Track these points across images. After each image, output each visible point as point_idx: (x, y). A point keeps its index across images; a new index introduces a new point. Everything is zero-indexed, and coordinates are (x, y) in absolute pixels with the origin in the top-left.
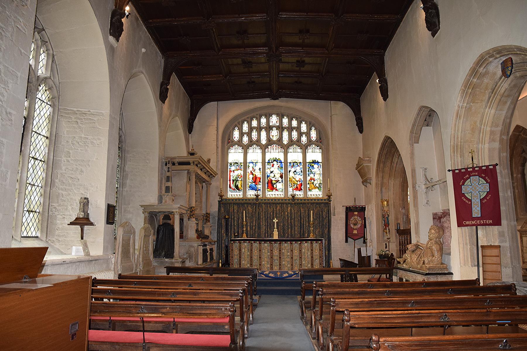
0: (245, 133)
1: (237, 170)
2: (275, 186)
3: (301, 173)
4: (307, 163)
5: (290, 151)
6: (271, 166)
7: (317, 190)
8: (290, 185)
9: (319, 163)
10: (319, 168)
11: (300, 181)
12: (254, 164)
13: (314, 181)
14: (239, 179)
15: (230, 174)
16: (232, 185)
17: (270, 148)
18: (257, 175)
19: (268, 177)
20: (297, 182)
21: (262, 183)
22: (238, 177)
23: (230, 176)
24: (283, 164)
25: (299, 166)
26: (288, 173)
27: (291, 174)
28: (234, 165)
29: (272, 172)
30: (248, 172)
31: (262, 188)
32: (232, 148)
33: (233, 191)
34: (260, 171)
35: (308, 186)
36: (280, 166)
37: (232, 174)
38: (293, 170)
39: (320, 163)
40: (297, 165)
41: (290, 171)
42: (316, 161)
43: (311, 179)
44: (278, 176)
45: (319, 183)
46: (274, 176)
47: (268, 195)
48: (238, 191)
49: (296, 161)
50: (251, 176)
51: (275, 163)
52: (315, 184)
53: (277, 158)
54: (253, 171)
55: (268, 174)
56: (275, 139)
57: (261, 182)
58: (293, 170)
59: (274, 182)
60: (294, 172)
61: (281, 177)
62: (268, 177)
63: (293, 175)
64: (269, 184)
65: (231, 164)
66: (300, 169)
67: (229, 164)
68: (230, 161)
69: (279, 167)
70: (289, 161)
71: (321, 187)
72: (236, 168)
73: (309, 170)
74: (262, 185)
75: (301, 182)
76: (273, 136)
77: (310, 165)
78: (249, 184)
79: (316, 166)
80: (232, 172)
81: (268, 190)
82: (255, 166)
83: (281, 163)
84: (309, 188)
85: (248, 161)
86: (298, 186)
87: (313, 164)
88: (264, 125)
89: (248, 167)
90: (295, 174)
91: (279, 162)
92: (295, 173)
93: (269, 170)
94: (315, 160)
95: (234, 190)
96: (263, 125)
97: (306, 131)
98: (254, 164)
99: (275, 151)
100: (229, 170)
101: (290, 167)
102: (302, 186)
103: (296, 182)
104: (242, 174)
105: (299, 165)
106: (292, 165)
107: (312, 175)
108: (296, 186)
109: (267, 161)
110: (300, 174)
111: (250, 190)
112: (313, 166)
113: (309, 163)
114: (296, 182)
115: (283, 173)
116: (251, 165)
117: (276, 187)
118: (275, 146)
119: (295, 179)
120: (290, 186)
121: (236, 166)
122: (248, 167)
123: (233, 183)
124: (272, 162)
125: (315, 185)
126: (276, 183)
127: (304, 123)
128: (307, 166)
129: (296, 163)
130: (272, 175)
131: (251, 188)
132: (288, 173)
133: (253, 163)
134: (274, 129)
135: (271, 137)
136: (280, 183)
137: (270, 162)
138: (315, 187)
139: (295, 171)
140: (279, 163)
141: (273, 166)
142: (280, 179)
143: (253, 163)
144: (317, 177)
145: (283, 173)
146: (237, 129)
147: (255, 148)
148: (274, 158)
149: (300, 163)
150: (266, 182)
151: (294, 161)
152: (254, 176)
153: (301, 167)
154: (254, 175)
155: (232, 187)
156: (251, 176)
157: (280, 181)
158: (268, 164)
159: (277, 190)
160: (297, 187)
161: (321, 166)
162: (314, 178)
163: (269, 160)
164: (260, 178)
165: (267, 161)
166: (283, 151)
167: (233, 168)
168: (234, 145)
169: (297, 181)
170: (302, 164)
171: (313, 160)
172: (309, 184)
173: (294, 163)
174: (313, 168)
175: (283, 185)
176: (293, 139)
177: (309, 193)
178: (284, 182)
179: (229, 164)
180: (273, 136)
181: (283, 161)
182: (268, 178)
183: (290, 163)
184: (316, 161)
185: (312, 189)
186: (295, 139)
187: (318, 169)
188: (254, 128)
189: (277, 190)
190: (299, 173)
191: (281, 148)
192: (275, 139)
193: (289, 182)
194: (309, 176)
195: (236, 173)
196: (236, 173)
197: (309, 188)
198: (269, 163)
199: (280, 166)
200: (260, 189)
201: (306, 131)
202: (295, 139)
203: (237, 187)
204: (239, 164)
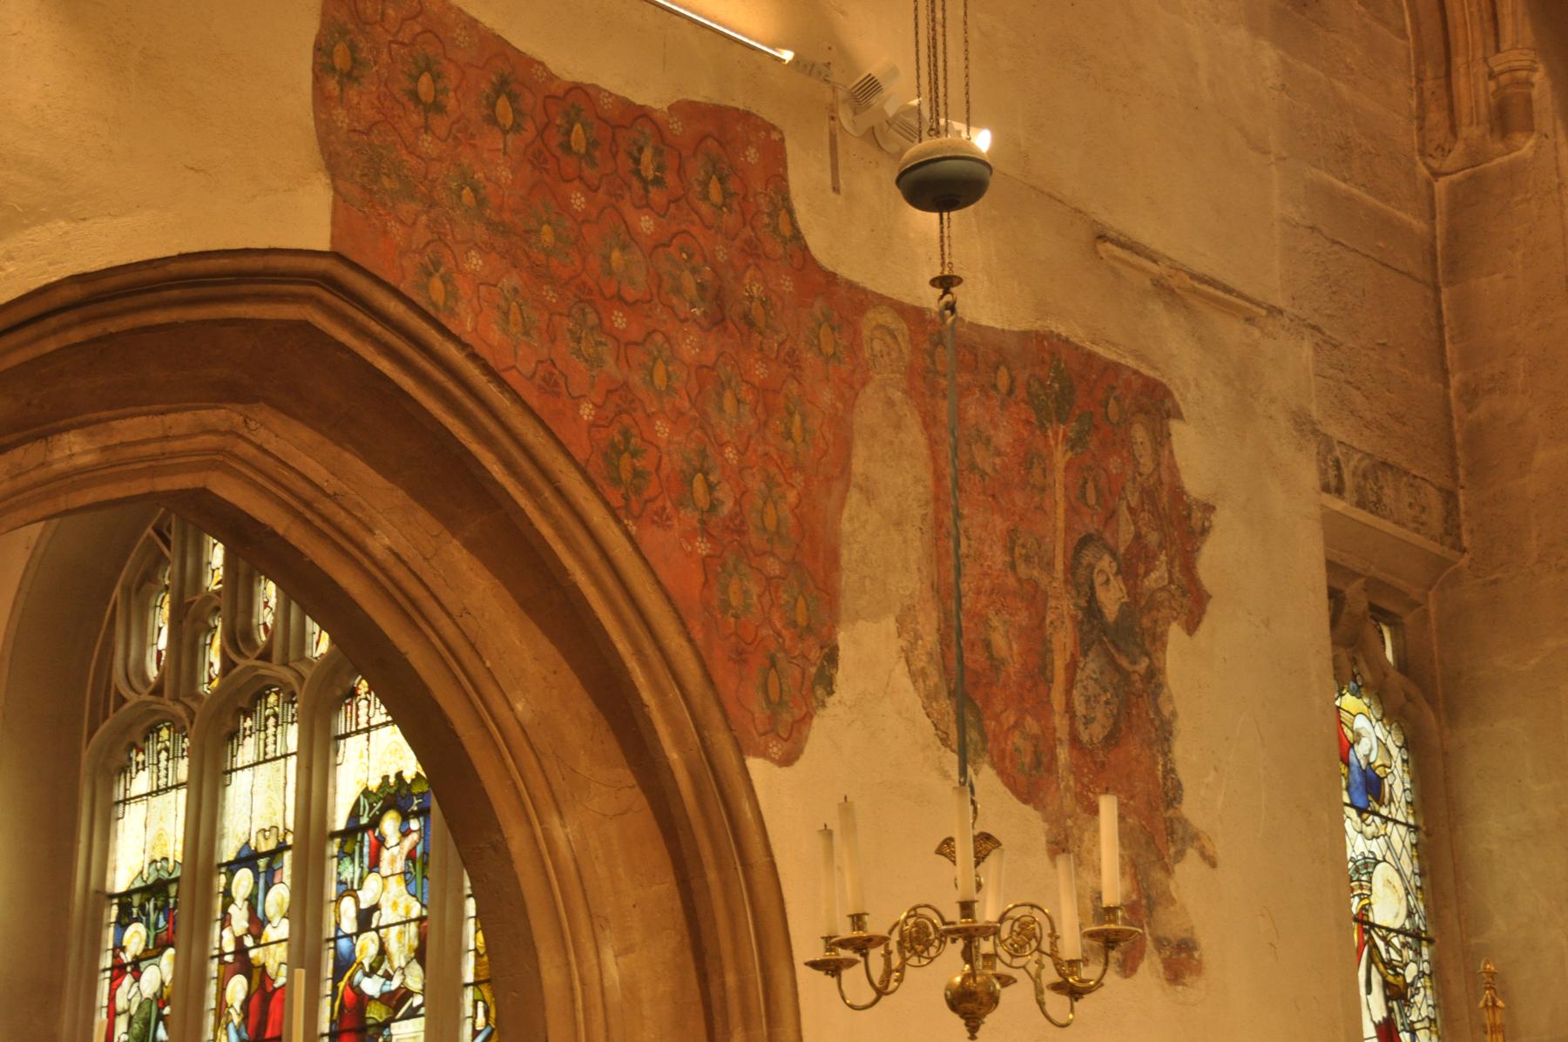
8: (481, 1020)
12: (262, 863)
15: (112, 998)
23: (113, 1014)
28: (142, 907)
32: (141, 757)
37: (127, 995)
44: (401, 943)
46: (383, 952)
54: (249, 942)
59: (375, 1013)
69: (411, 856)
72: (152, 934)
80: (128, 979)
98: (262, 863)
100: (107, 961)
116: (244, 880)
121: (153, 917)
126: (386, 1024)
136: (413, 1013)
147: (272, 721)
152: (255, 986)
156: (238, 988)
163: (355, 814)
167: (136, 938)
182: (342, 985)
198: (353, 831)
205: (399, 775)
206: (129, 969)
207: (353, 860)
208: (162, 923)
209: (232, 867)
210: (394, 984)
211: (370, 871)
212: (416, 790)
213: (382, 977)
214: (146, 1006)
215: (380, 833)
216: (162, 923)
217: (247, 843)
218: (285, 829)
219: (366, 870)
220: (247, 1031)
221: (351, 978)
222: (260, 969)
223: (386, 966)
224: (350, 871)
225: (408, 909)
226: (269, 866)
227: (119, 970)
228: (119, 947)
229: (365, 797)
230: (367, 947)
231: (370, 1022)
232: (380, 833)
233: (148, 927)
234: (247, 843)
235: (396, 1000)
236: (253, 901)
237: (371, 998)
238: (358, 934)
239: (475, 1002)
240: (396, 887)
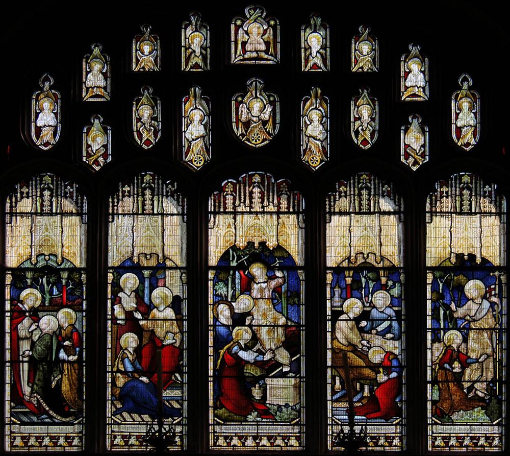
0: (94, 109)
1: (54, 307)
2: (256, 393)
3: (395, 324)
4: (430, 277)
5: (343, 204)
6: (238, 287)
7: (478, 414)
8: (338, 385)
9: (494, 268)
10: (494, 299)
11: (388, 370)
13: (465, 365)
14: (62, 355)
15: (14, 328)
16: (27, 390)
17: (229, 189)
18: (159, 332)
19: (220, 341)
20: (372, 375)
21: (186, 377)
22: (60, 346)
23: (16, 339)
24: (302, 275)
25: (385, 287)
26: (329, 324)
27: (344, 331)
29: (239, 319)
30: (114, 319)
31: (185, 404)
33: (35, 419)
34: (177, 310)
35: (432, 393)
36: (284, 289)
37: (25, 325)
38: (354, 306)
39: (497, 273)
40: (378, 279)
41: (336, 315)
42: (479, 260)
43: (450, 355)
45: (490, 376)
46: (255, 339)
47: (221, 441)
48: (59, 418)
49: (371, 260)
50: (130, 340)
51: (257, 270)
52: (466, 385)
53: (271, 243)
54: (138, 316)
55: (222, 330)
56: (257, 139)
57: (185, 369)
58: (354, 306)
60: (357, 320)
61: (290, 344)
62: (220, 341)
63: (355, 338)
64: (227, 384)
65: (18, 273)
66: (391, 306)
67: (9, 279)
68: (12, 261)
69: (277, 290)
70: (333, 258)
71: (500, 402)
73: (435, 310)
74: (185, 388)
75: (394, 375)
76: (247, 124)
77: (447, 284)
78: (121, 381)
79: (473, 287)
80: (26, 322)
81: (221, 412)
82: (152, 288)
83: (288, 264)
84: (434, 402)
85: (114, 260)
86: (379, 393)
87: (462, 278)
88: (200, 62)
89: (115, 294)
90: (362, 330)
91: (281, 268)
92: (364, 323)
93: (222, 307)
94: (472, 257)
95: (39, 411)
96: (193, 62)
97: (423, 97)
98: (146, 273)
99: (257, 208)
101: (337, 291)
102: (399, 393)
103: (367, 372)
104: (82, 325)
105: (384, 280)
106: (349, 280)
107: (454, 337)
108: (366, 393)
109: (213, 261)
110: (389, 329)
111: (125, 414)
112: (460, 288)
113: (438, 274)
114: (367, 372)
115: (298, 325)
116: (130, 281)
117: (264, 397)
118: (257, 179)
119: (363, 355)
120: (334, 392)
122: (115, 294)
123: (31, 381)
124: (241, 267)
125: (470, 389)
126: (263, 377)
127: (414, 50)
128: (429, 288)
129: (374, 270)
130: (243, 334)
131: (131, 405)
132: (329, 324)
133: (136, 269)
134: (254, 84)
135: (239, 132)
136: (283, 375)
137: (234, 264)
138: (470, 402)
139: (365, 315)
140: (279, 274)
141: (246, 289)
142: (283, 356)
143: (136, 269)
144: (477, 345)
145: (303, 322)
146: (47, 84)
148: (251, 244)
149: (392, 270)
150: (211, 373)
151: (360, 260)
152: (145, 341)
153: (396, 291)
154: (146, 337)
155: (27, 398)
156: (130, 340)
157: (286, 369)
158: (216, 280)
159: (266, 413)
160: (373, 398)
161: (504, 288)
162: (463, 348)
163: (225, 257)
164: (177, 351)
165: (213, 261)
166: (303, 205)
167: (31, 297)
168: (38, 172)
169: (375, 368)
170: (402, 277)
171: (460, 256)
172: (434, 382)
173: (358, 270)
174: (462, 299)
175: (297, 387)
176: (358, 141)
177: (437, 432)
178: (303, 373)
179: (9, 279)
180: (247, 124)
181: (299, 260)
182: (222, 352)
183: (338, 271)
184: (479, 260)
185: (453, 409)
186: (365, 142)
187: (486, 304)
188: (145, 77)
189: (266, 413)
190: (386, 324)
191: (291, 189)
192: (257, 139)
193: (329, 371)
194: (436, 339)
195: (48, 323)
196: (48, 323)
197: (434, 402)
199: (284, 289)
200: (176, 406)
201: (423, 97)
202: (365, 142)
203: (53, 397)
204: (65, 275)
205: (263, 244)
206: (27, 314)
207: (227, 285)
208: (55, 291)
209: (121, 270)
210: (268, 357)
211: (242, 293)
212: (278, 254)
213: (256, 352)
214: (47, 338)
215: (249, 272)
216: (55, 291)
217: (131, 259)
218: (164, 256)
219: (238, 292)
220: (140, 365)
221: (228, 349)
222: (150, 333)
223: (258, 346)
224: (222, 290)
225: (276, 319)
226: (152, 276)
227: (18, 315)
228: (15, 300)
229: (233, 251)
230: (243, 334)
231: (247, 374)
232: (249, 272)
233: (42, 291)
234: (131, 259)
235: (270, 368)
236: (140, 293)
237: (248, 362)
238: (234, 326)
239: (333, 378)
240: (263, 305)
